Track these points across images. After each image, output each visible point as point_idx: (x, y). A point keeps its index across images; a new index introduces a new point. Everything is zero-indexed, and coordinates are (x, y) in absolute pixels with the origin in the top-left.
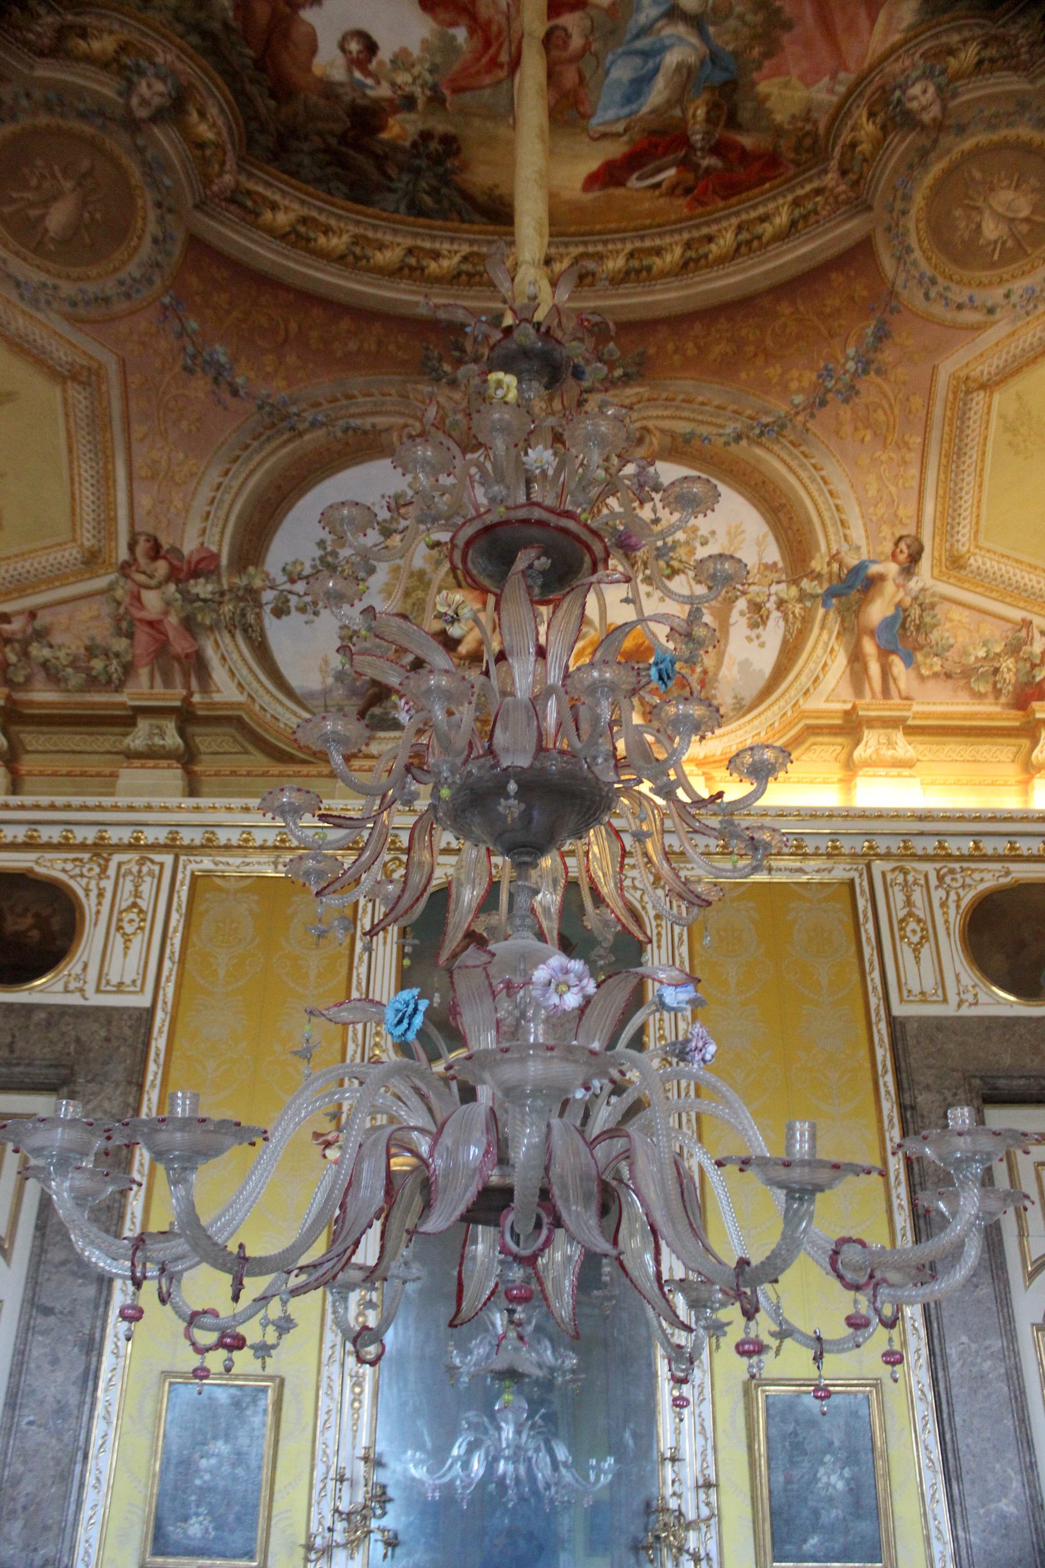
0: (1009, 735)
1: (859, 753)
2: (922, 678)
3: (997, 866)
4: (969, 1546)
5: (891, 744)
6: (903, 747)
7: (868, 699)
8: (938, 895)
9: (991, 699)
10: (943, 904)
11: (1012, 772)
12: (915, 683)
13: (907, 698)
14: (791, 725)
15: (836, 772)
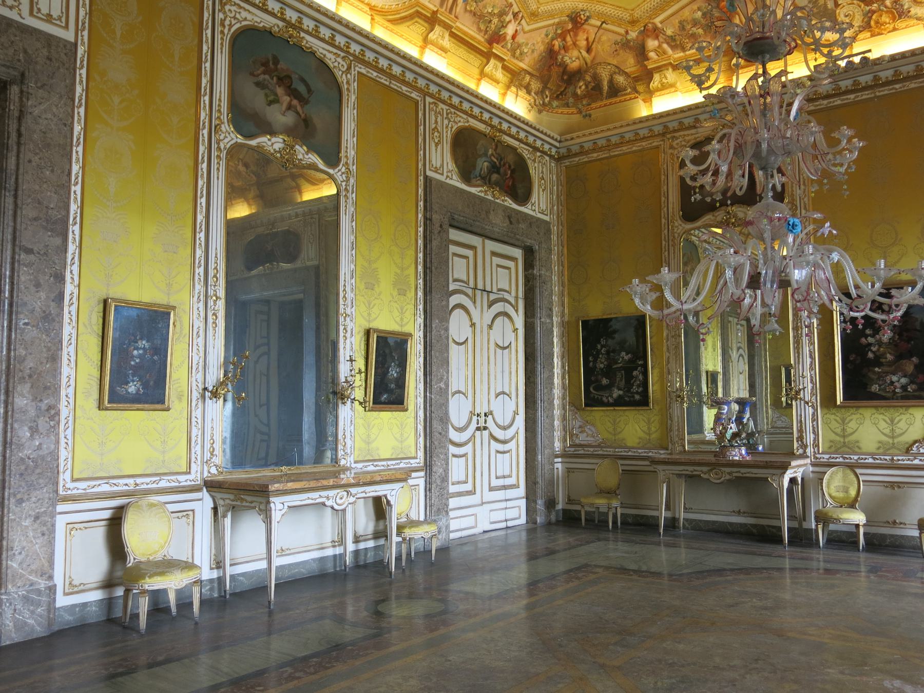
0: (481, 55)
1: (432, 36)
2: (466, 10)
3: (465, 116)
4: (431, 399)
5: (443, 37)
6: (447, 42)
7: (443, 10)
8: (446, 122)
9: (482, 34)
10: (447, 127)
11: (476, 72)
12: (462, 11)
13: (456, 17)
14: (411, 7)
15: (419, 41)
